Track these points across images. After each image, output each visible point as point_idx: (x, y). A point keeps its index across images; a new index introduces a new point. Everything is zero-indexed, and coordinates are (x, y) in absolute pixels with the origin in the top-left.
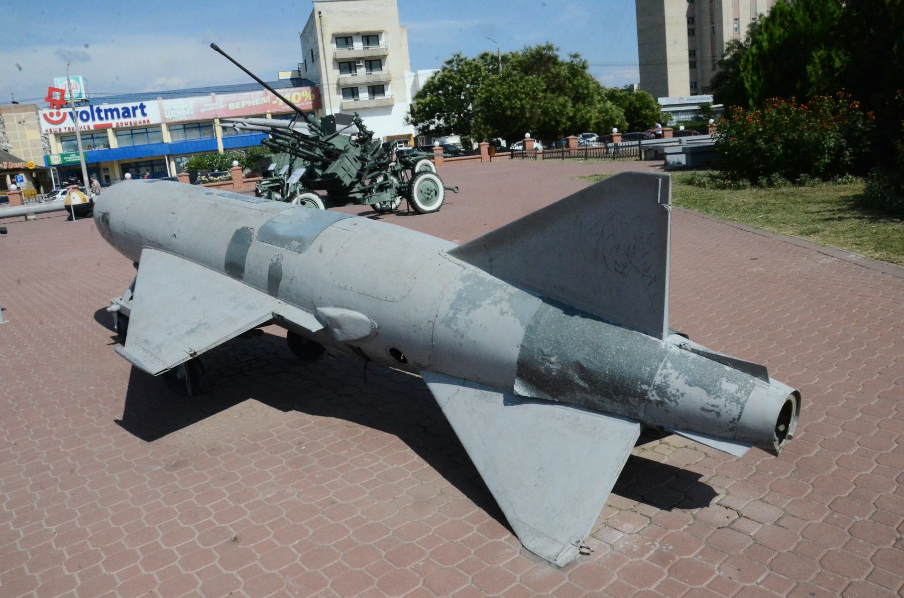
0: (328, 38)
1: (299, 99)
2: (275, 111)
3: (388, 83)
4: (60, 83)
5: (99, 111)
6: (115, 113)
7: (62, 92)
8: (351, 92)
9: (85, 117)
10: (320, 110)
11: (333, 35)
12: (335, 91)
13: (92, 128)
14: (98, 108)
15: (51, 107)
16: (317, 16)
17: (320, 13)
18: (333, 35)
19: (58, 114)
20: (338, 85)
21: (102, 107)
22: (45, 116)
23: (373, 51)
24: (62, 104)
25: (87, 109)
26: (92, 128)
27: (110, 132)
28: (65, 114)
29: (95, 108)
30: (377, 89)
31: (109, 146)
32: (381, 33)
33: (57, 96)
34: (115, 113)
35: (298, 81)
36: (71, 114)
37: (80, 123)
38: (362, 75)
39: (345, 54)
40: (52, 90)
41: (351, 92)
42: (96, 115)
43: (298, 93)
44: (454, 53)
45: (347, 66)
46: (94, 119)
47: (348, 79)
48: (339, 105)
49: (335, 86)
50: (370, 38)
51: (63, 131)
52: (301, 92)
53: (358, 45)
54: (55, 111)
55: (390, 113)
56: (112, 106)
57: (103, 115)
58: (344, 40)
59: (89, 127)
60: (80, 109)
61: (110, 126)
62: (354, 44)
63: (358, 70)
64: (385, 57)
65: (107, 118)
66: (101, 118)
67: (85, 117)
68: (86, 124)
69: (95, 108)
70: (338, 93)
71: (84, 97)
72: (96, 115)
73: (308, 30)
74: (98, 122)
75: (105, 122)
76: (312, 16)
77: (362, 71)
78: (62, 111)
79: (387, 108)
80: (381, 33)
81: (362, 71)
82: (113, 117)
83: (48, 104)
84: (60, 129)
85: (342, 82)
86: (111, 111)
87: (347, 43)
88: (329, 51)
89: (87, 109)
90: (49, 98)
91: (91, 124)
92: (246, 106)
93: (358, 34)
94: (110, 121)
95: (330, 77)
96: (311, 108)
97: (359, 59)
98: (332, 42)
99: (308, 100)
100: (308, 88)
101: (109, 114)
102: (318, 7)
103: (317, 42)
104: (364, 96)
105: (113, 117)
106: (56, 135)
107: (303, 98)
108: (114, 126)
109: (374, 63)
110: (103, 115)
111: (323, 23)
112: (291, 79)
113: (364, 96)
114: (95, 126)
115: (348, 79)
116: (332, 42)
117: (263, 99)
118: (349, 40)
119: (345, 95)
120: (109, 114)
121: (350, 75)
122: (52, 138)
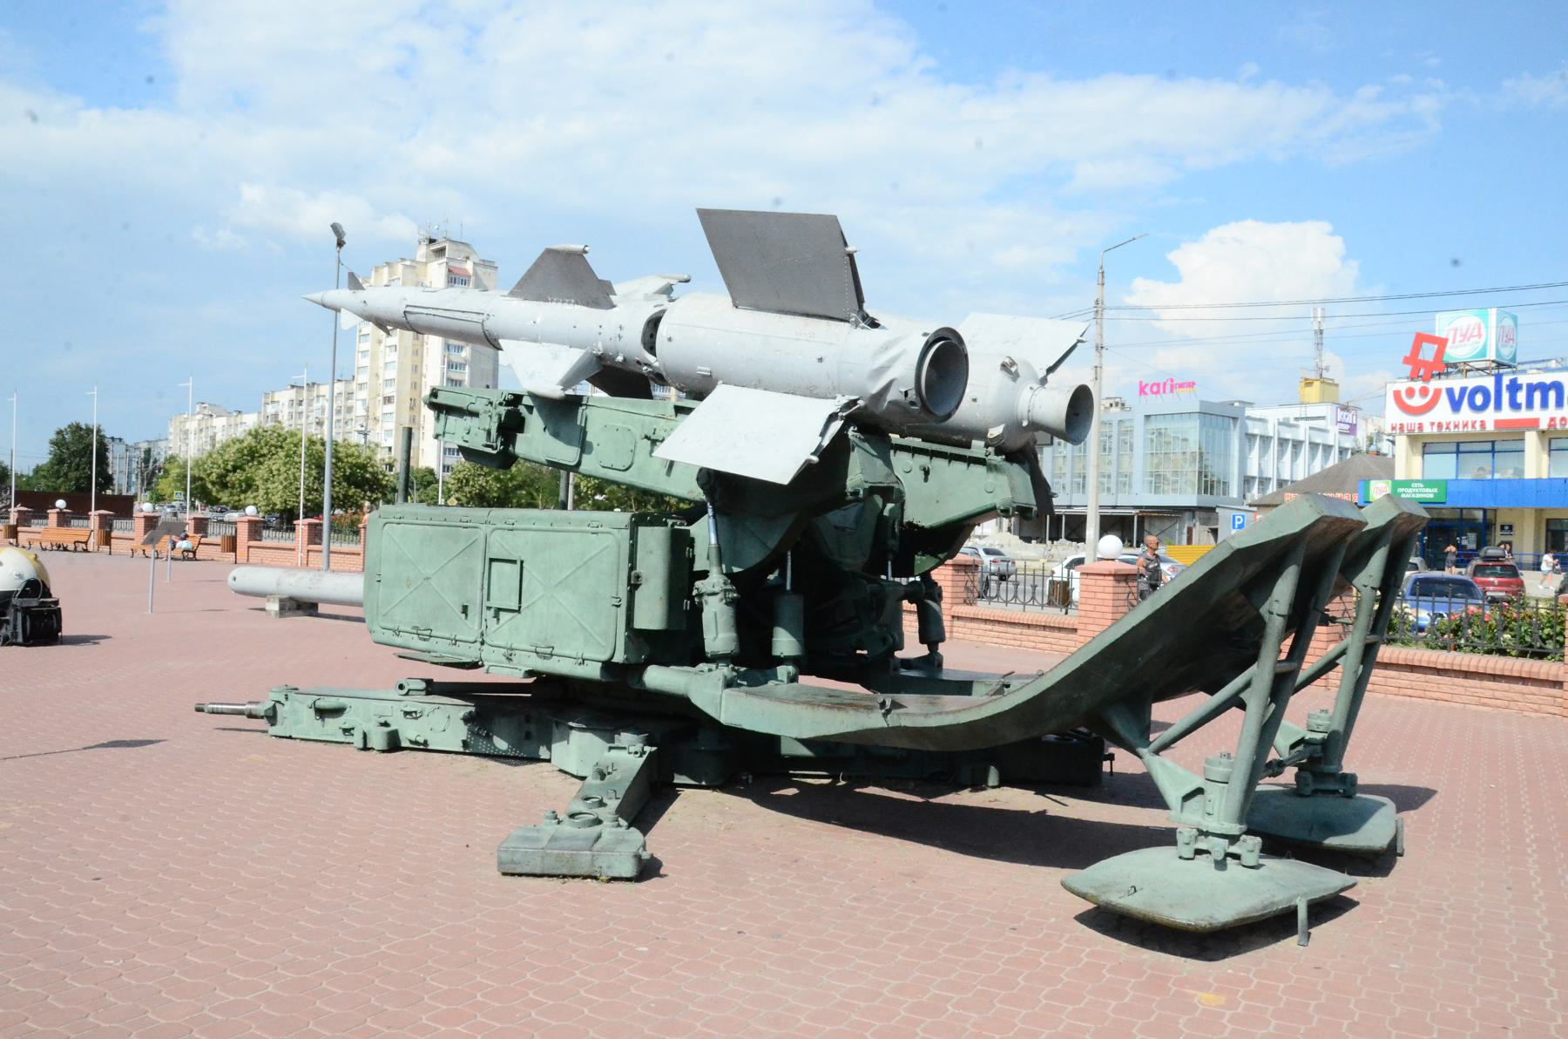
4: (1443, 325)
5: (1514, 387)
6: (1552, 395)
7: (1442, 343)
9: (1479, 399)
13: (1490, 427)
14: (1513, 382)
15: (1413, 377)
19: (1424, 392)
21: (1523, 380)
22: (1397, 394)
24: (1444, 368)
25: (1489, 383)
26: (1490, 427)
27: (1531, 438)
28: (1437, 393)
29: (1506, 381)
31: (1522, 472)
33: (1428, 352)
34: (1552, 395)
36: (1450, 392)
37: (1466, 413)
40: (1421, 339)
42: (1506, 396)
46: (1498, 406)
51: (1427, 430)
54: (1417, 385)
56: (1548, 378)
57: (1521, 397)
59: (1483, 424)
60: (1471, 382)
61: (1533, 423)
65: (1530, 405)
66: (1515, 405)
67: (1479, 399)
68: (1478, 417)
69: (1506, 381)
71: (1492, 355)
72: (1506, 396)
74: (1507, 413)
75: (1524, 414)
78: (1434, 384)
82: (1544, 404)
83: (1408, 369)
84: (1421, 426)
86: (1544, 388)
89: (1489, 383)
90: (1413, 359)
91: (1490, 418)
94: (1537, 412)
101: (1537, 396)
105: (1544, 404)
106: (1413, 438)
108: (1544, 425)
110: (1521, 397)
114: (1497, 423)
120: (1537, 396)
122: (1402, 441)
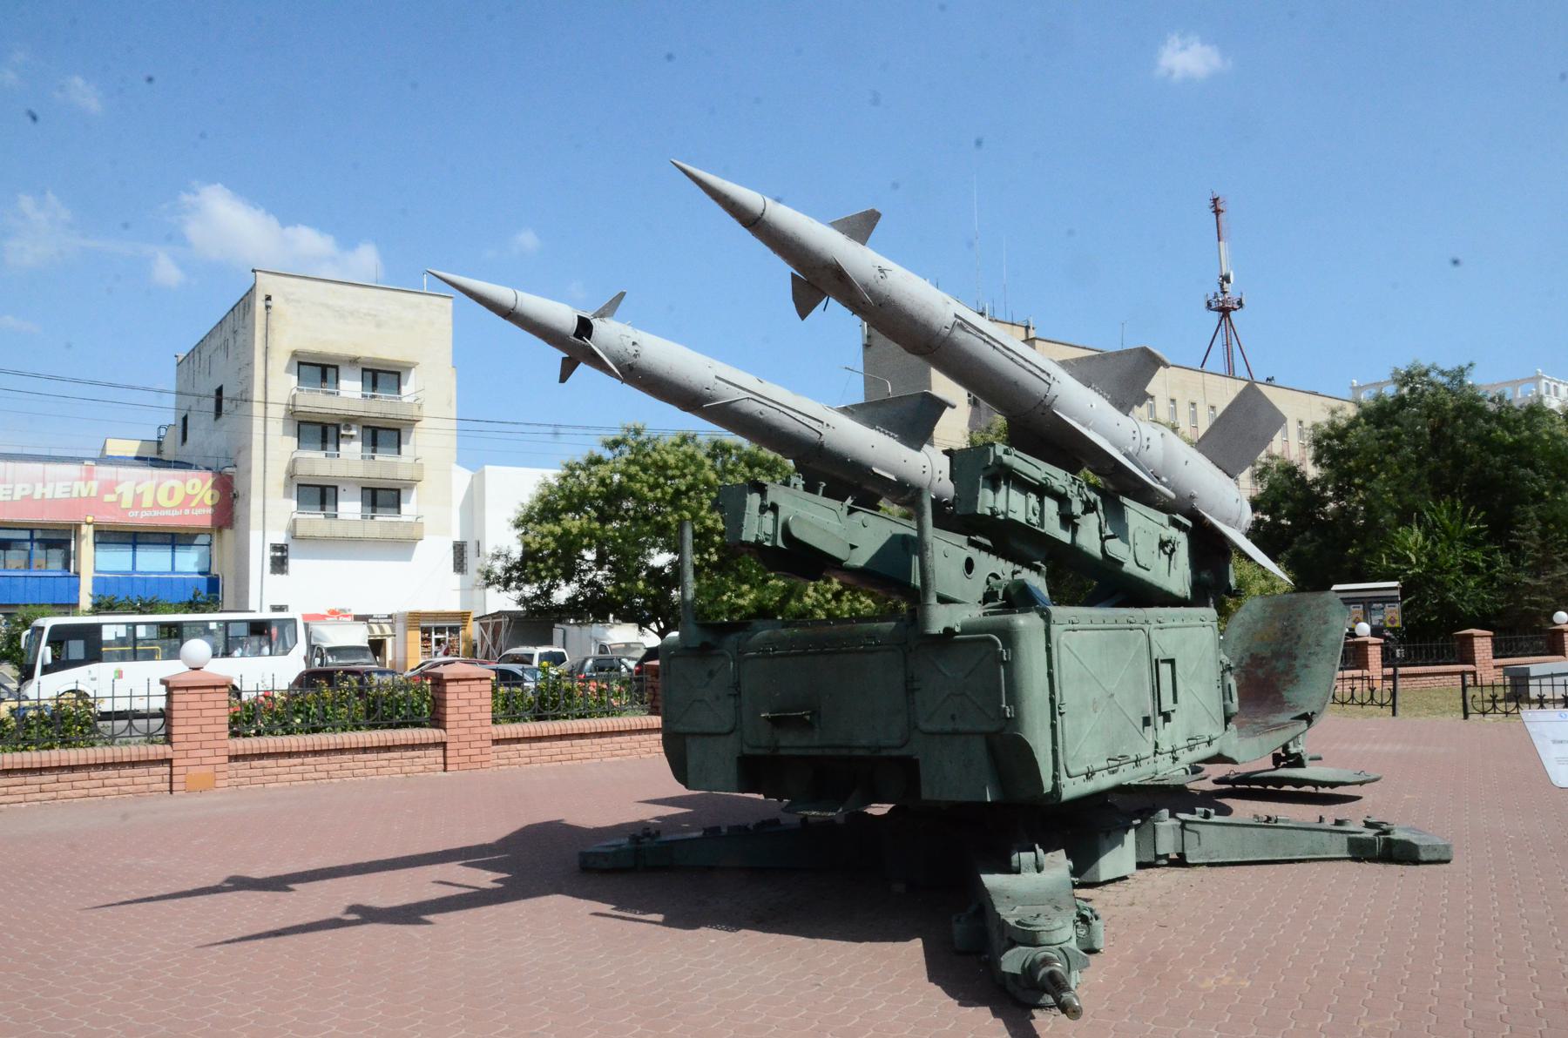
0: (280, 360)
1: (178, 498)
2: (109, 518)
3: (411, 484)
8: (321, 495)
10: (227, 533)
11: (295, 354)
12: (281, 490)
16: (260, 305)
17: (268, 298)
18: (295, 354)
20: (291, 475)
23: (382, 406)
30: (383, 497)
32: (409, 367)
35: (155, 459)
38: (351, 460)
39: (318, 401)
41: (321, 495)
43: (177, 483)
44: (630, 424)
45: (321, 431)
47: (318, 463)
48: (285, 522)
49: (282, 477)
50: (381, 376)
52: (185, 482)
53: (350, 393)
55: (408, 558)
58: (320, 370)
62: (342, 383)
63: (342, 446)
64: (412, 422)
70: (287, 495)
73: (216, 341)
76: (244, 305)
77: (352, 450)
79: (403, 545)
80: (409, 367)
81: (352, 450)
85: (302, 470)
87: (324, 378)
88: (277, 388)
92: (28, 499)
93: (354, 361)
95: (273, 454)
96: (207, 523)
97: (350, 421)
98: (288, 370)
99: (201, 504)
100: (209, 473)
102: (266, 284)
103: (250, 364)
104: (350, 507)
107: (188, 498)
109: (384, 434)
111: (273, 324)
112: (137, 458)
113: (350, 507)
115: (318, 463)
116: (288, 370)
117: (78, 485)
118: (331, 373)
119: (302, 501)
121: (322, 454)
